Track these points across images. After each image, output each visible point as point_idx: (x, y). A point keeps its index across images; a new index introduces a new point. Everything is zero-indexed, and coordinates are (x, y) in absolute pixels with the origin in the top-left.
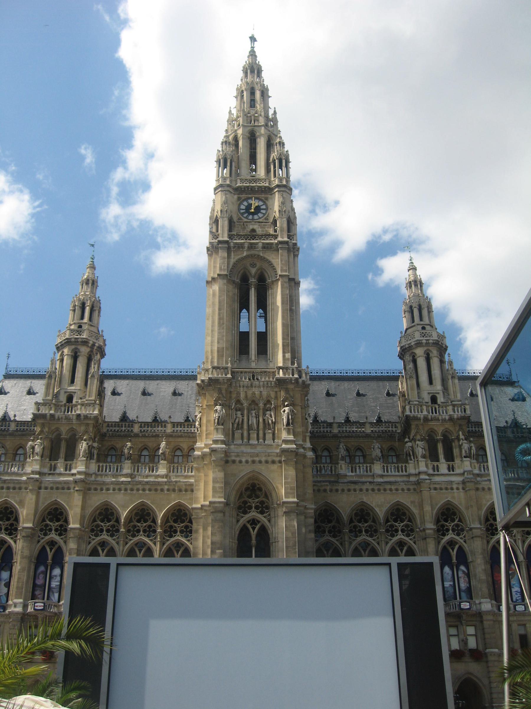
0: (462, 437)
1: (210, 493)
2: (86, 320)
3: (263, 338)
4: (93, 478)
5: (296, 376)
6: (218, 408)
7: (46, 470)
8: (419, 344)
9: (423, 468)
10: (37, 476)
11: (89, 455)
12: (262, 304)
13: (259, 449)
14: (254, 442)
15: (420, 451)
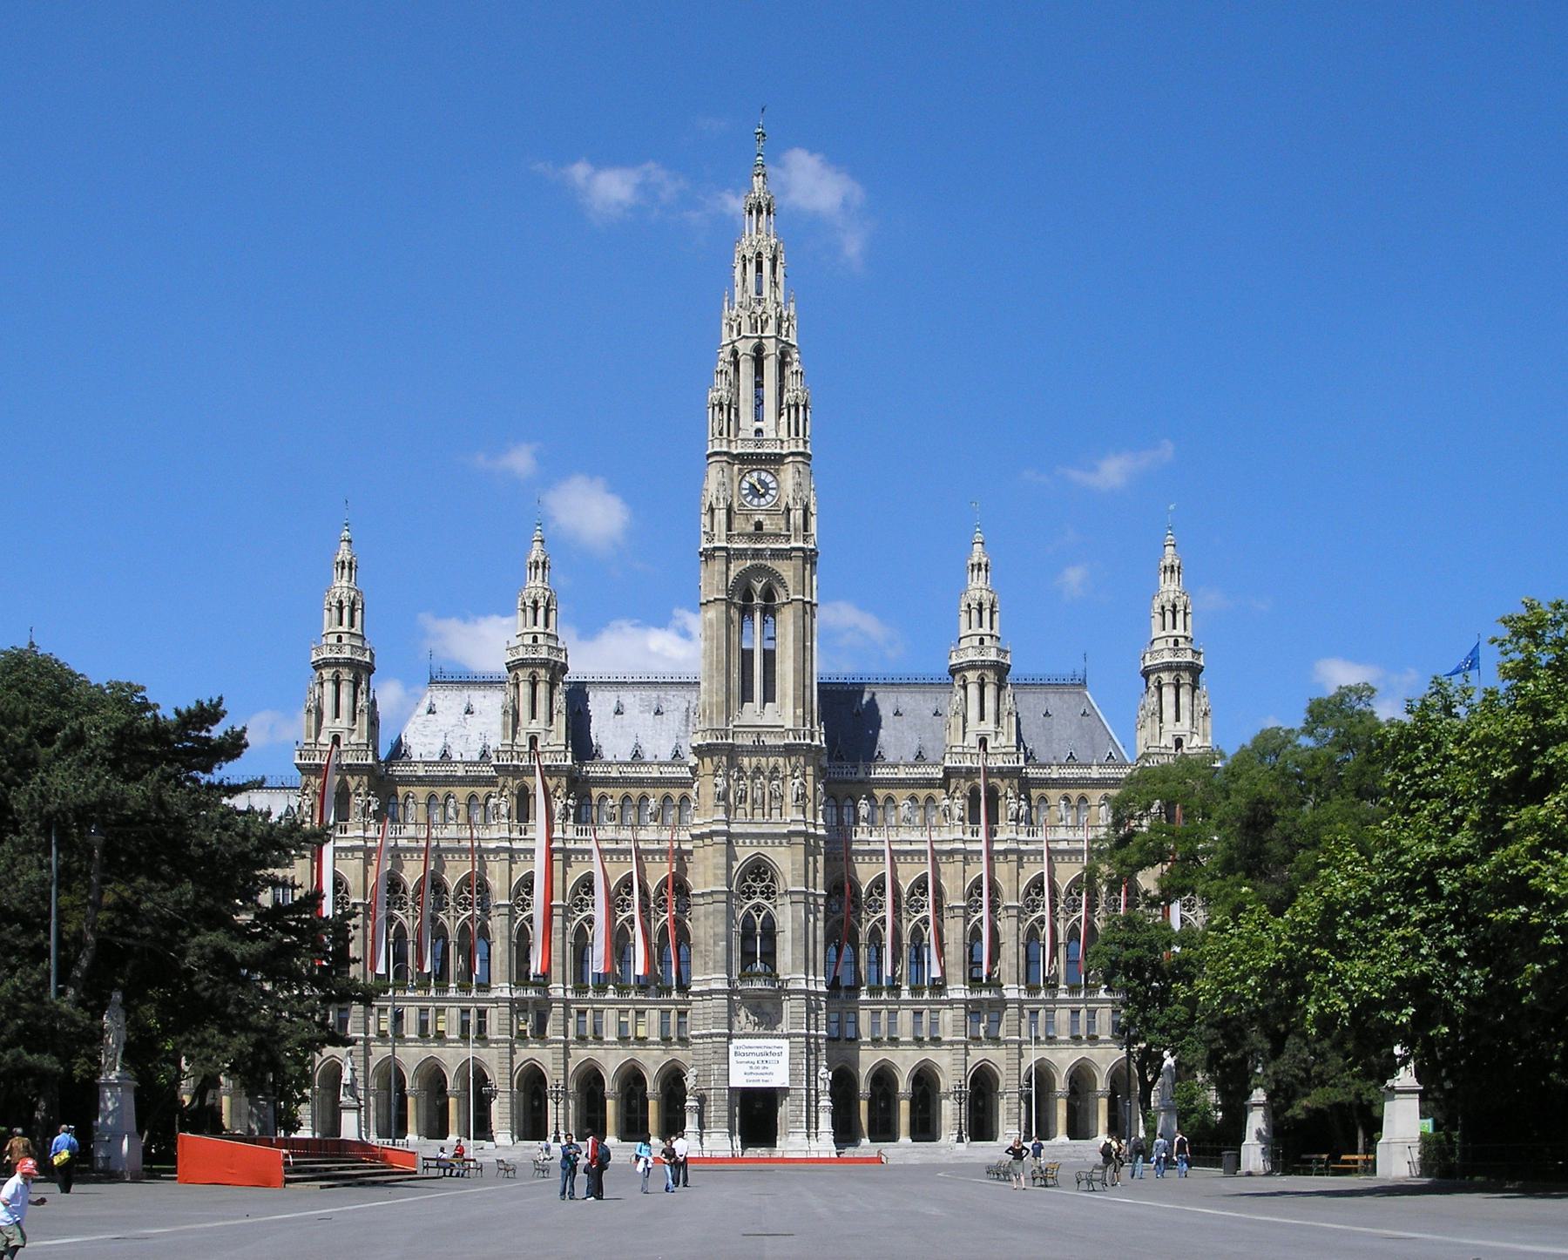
0: (1010, 794)
1: (710, 878)
2: (540, 628)
3: (769, 657)
4: (570, 846)
5: (808, 741)
6: (719, 780)
7: (515, 835)
8: (972, 666)
9: (960, 835)
10: (507, 844)
11: (566, 817)
12: (769, 611)
13: (765, 829)
14: (758, 818)
15: (957, 812)
